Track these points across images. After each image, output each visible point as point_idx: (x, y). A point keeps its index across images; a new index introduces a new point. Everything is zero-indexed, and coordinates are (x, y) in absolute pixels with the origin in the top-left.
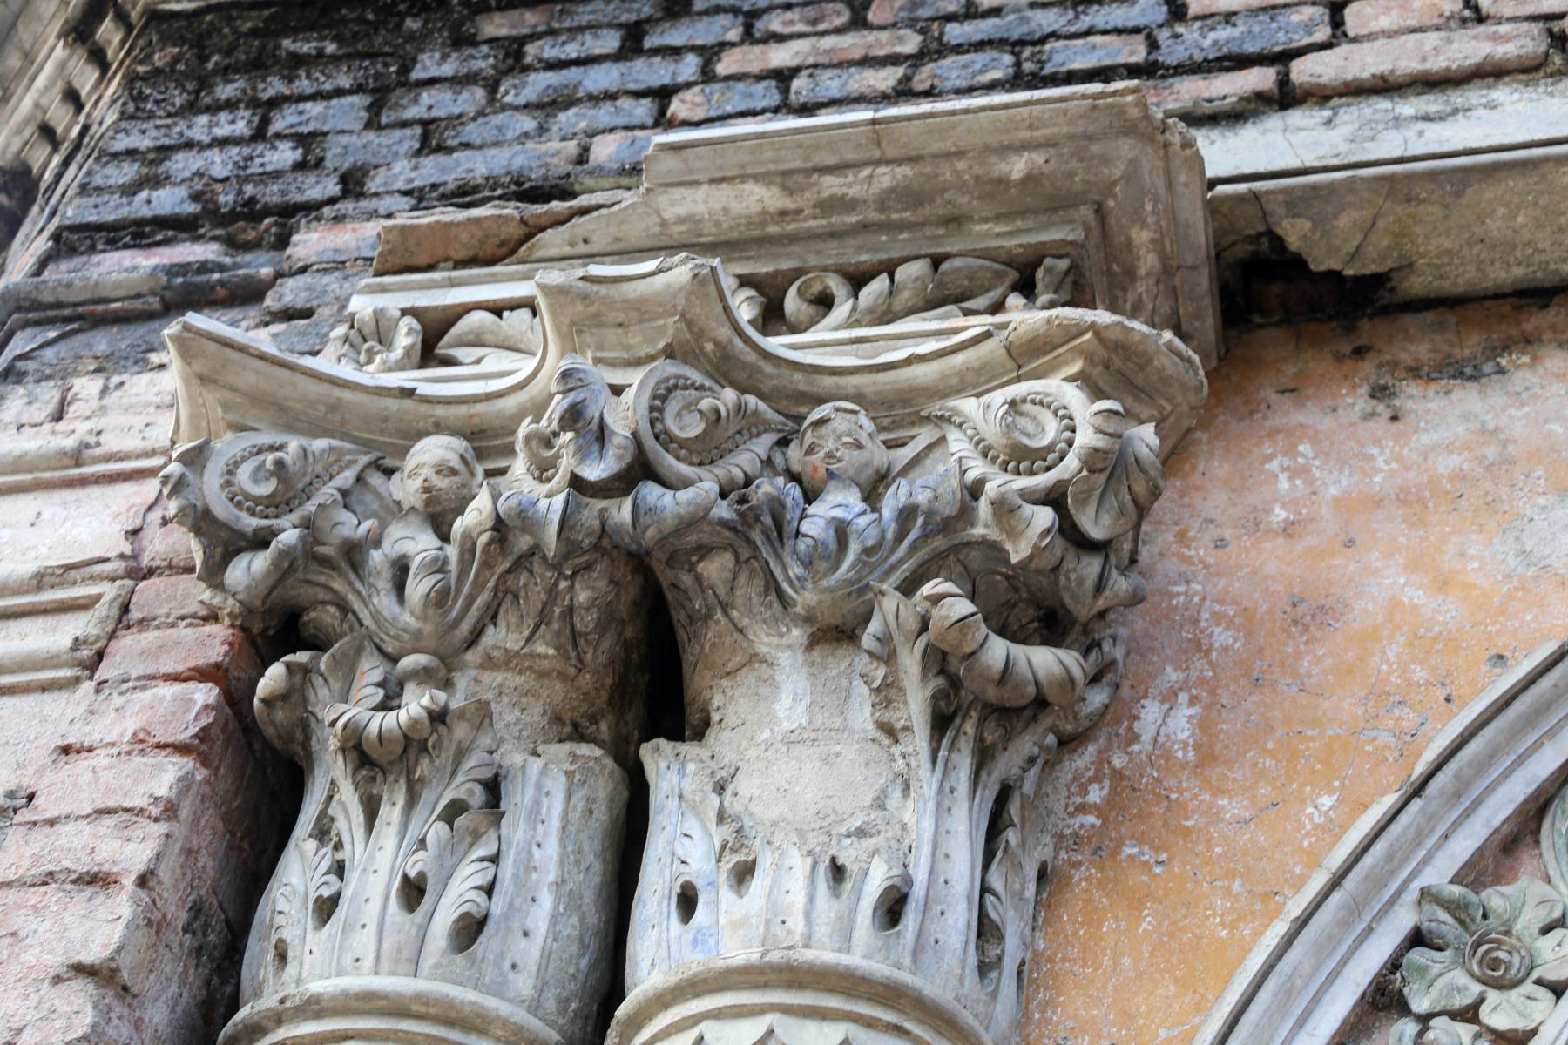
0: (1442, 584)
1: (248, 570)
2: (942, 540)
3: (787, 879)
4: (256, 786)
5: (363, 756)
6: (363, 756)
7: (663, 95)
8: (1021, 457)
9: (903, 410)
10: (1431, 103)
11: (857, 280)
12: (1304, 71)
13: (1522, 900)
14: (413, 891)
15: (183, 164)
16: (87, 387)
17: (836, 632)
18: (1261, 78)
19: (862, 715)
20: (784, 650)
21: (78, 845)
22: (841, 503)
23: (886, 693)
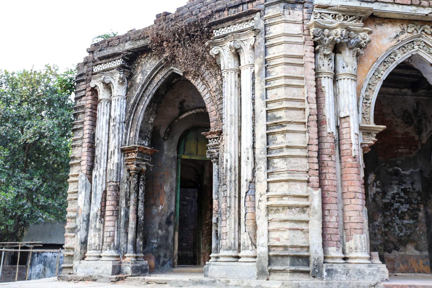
0: (378, 44)
8: (364, 39)
10: (384, 4)
11: (350, 16)
14: (328, 65)
16: (291, 11)
19: (352, 55)
20: (347, 49)
23: (353, 54)
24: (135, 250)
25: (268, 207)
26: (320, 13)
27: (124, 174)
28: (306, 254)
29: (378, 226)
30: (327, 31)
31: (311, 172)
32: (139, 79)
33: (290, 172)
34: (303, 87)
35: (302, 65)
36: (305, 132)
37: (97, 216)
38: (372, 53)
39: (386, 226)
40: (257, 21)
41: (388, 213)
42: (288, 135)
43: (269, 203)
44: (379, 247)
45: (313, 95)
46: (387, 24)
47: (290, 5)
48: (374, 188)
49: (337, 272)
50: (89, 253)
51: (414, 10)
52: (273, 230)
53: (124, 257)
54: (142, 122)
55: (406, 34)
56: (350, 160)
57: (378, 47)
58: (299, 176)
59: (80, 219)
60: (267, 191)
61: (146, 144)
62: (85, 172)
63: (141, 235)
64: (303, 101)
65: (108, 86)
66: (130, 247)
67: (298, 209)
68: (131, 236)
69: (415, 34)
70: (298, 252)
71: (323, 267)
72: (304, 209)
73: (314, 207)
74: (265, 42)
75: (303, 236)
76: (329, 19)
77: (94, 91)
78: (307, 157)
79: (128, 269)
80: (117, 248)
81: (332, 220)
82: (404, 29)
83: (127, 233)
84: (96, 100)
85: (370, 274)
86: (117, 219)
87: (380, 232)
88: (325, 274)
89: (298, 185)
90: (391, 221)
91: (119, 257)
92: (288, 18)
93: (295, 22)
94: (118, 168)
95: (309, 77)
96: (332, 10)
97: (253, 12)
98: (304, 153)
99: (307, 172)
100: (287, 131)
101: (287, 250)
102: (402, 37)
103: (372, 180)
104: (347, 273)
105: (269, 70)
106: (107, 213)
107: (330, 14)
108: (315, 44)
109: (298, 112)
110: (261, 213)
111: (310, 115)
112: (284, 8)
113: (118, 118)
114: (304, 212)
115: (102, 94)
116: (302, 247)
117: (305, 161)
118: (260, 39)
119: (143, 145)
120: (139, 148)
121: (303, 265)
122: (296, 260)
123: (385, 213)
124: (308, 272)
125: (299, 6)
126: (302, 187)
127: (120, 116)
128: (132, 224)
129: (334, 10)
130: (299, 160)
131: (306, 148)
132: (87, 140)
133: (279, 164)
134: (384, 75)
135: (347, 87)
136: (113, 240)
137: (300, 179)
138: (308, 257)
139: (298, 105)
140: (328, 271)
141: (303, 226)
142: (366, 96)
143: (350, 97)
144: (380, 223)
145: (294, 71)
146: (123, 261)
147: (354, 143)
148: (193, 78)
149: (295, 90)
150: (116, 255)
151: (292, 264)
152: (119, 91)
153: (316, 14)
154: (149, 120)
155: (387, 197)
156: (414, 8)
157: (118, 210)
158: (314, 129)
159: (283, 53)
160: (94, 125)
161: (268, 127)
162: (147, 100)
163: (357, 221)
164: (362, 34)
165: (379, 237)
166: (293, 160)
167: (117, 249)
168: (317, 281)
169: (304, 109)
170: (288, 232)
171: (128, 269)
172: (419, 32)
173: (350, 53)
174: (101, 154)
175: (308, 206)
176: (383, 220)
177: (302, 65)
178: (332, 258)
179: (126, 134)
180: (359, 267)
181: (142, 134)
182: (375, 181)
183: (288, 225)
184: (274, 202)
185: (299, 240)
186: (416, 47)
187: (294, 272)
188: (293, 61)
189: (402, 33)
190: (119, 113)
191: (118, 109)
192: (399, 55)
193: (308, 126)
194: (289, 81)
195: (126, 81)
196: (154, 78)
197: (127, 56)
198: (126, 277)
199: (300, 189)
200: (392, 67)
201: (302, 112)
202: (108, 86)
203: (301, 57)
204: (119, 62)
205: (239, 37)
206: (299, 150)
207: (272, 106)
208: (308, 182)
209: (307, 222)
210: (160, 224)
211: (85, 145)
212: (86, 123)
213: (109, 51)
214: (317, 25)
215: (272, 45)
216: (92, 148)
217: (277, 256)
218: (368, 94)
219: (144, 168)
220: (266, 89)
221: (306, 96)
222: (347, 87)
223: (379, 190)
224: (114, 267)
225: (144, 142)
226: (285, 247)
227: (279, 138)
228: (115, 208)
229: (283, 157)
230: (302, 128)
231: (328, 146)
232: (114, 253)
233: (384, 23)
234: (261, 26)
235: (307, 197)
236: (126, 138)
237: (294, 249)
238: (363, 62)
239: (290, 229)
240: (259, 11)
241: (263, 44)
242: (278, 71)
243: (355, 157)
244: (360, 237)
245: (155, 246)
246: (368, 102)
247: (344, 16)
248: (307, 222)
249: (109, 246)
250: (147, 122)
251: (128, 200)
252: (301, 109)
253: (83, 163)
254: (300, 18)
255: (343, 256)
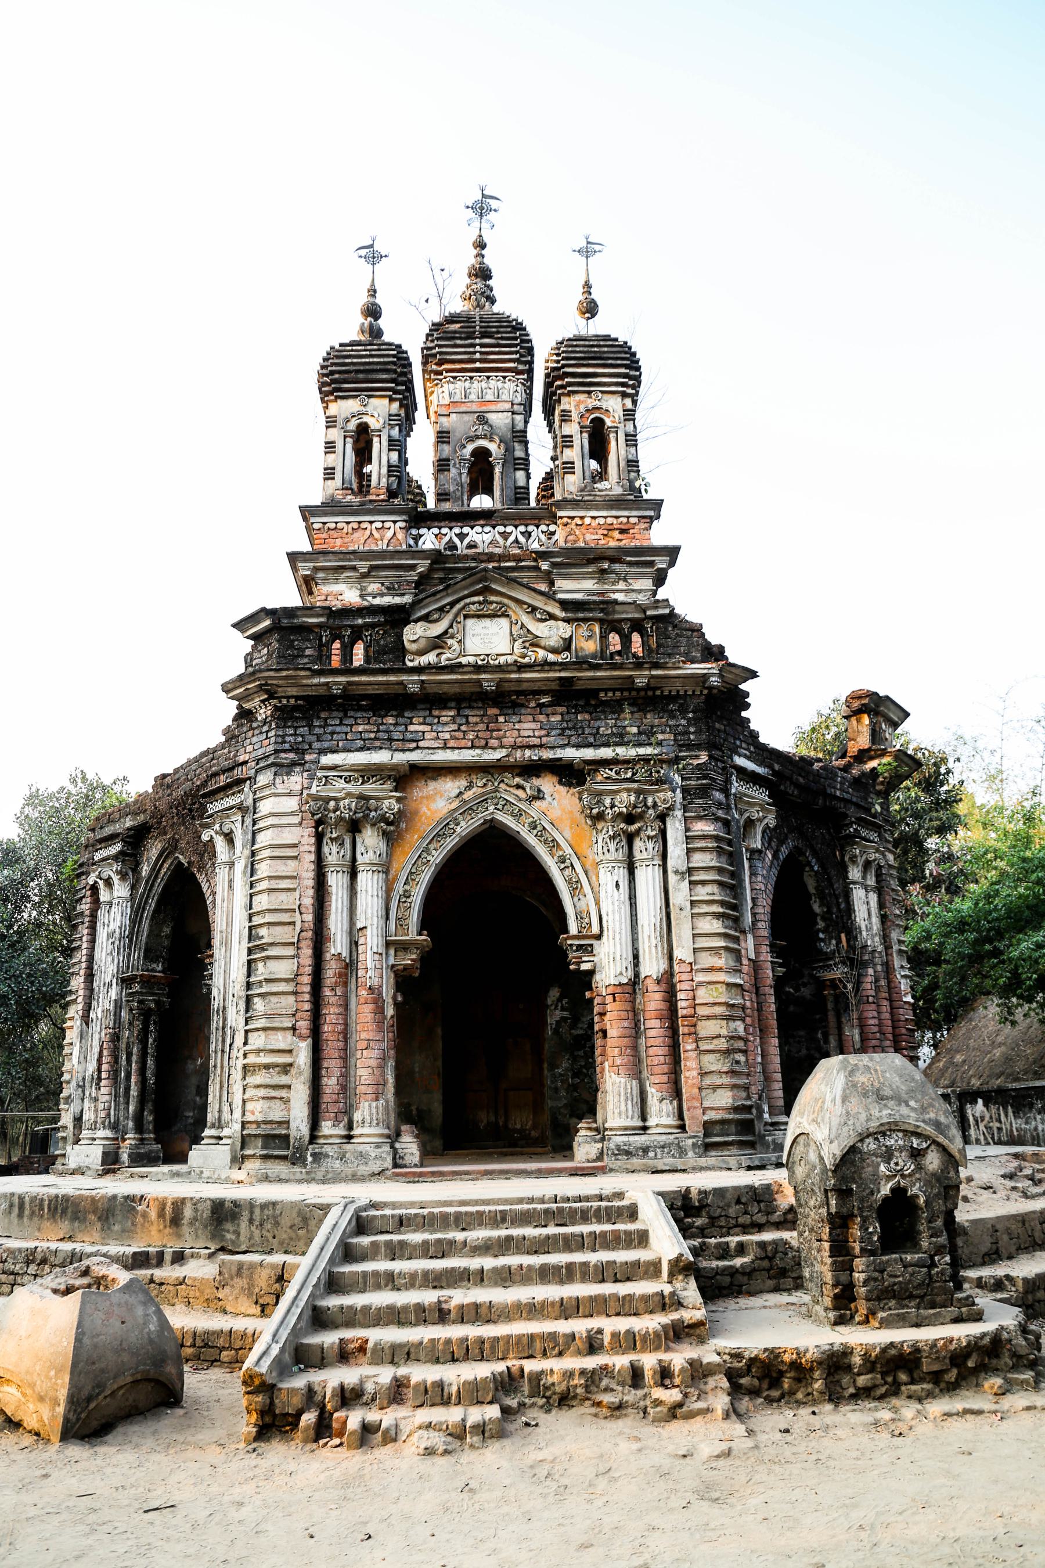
1: (317, 817)
2: (383, 819)
3: (371, 853)
4: (319, 838)
5: (331, 838)
6: (331, 838)
7: (346, 733)
9: (378, 799)
10: (430, 751)
11: (373, 776)
12: (421, 744)
13: (431, 847)
15: (288, 739)
16: (285, 778)
17: (373, 825)
18: (414, 745)
21: (307, 848)
22: (373, 814)
24: (139, 1128)
25: (245, 1067)
26: (326, 777)
27: (124, 1014)
28: (284, 1132)
29: (561, 1075)
30: (332, 804)
31: (299, 1014)
32: (145, 870)
33: (269, 1016)
34: (294, 890)
35: (295, 858)
36: (293, 957)
37: (93, 1078)
38: (419, 824)
39: (575, 1075)
40: (246, 796)
41: (581, 1053)
42: (270, 963)
43: (246, 1061)
44: (562, 1110)
45: (308, 901)
46: (445, 776)
47: (285, 770)
48: (558, 1012)
49: (327, 1156)
50: (85, 1133)
51: (478, 755)
52: (251, 1100)
53: (124, 1140)
54: (148, 936)
55: (474, 789)
56: (364, 993)
57: (429, 813)
58: (281, 1022)
59: (73, 1084)
60: (245, 1044)
61: (160, 968)
62: (80, 1013)
63: (150, 1106)
64: (294, 910)
65: (108, 883)
66: (131, 1124)
67: (277, 1069)
68: (131, 1108)
69: (489, 787)
70: (274, 1129)
71: (307, 1149)
72: (286, 1069)
73: (299, 1067)
74: (254, 824)
75: (283, 1107)
76: (341, 784)
77: (94, 888)
78: (295, 993)
79: (125, 1157)
80: (114, 1127)
81: (330, 1083)
82: (471, 782)
83: (128, 1103)
84: (96, 902)
85: (376, 1157)
86: (116, 1083)
87: (565, 1086)
88: (310, 1159)
89: (280, 1035)
90: (584, 1067)
91: (117, 1139)
92: (280, 788)
93: (289, 794)
94: (116, 1007)
95: (305, 875)
96: (343, 771)
97: (240, 782)
98: (290, 988)
99: (294, 1015)
100: (268, 957)
101: (259, 1127)
102: (468, 795)
103: (555, 999)
104: (342, 1157)
105: (256, 866)
106: (104, 1075)
107: (341, 777)
108: (319, 823)
109: (286, 927)
110: (237, 1075)
111: (302, 931)
112: (275, 774)
113: (118, 930)
114: (286, 1073)
115: (104, 896)
116: (280, 1123)
117: (291, 999)
118: (248, 821)
119: (153, 970)
120: (141, 976)
121: (280, 1148)
122: (271, 1141)
123: (576, 1053)
124: (284, 1158)
125: (298, 769)
126: (285, 1037)
127: (120, 928)
128: (134, 1092)
129: (347, 771)
130: (283, 997)
131: (292, 980)
132: (84, 965)
133: (259, 1004)
134: (437, 857)
135: (369, 883)
136: (109, 1115)
137: (281, 1025)
138: (287, 1136)
139: (285, 917)
140: (314, 1155)
141: (283, 1093)
142: (405, 891)
143: (369, 898)
144: (566, 1069)
145: (283, 868)
146: (122, 1145)
147: (373, 967)
148: (198, 871)
149: (283, 896)
150: (111, 1136)
151: (263, 1148)
152: (121, 890)
153: (321, 779)
154: (161, 931)
155: (580, 1025)
156: (478, 751)
157: (117, 1070)
158: (307, 952)
159: (267, 843)
160: (93, 941)
161: (250, 951)
162: (152, 904)
163: (368, 1082)
164: (386, 802)
165: (563, 1093)
166: (274, 999)
167: (114, 1128)
168: (297, 1169)
169: (293, 923)
170: (261, 1101)
171: (125, 1157)
172: (496, 784)
173: (373, 832)
174: (99, 986)
175: (291, 1065)
176: (572, 1065)
177: (295, 858)
178: (326, 1137)
179: (129, 955)
180: (361, 1148)
181: (150, 954)
182: (560, 1000)
183: (262, 1092)
184: (252, 1059)
185: (277, 1115)
186: (491, 808)
187: (265, 1157)
188: (285, 852)
189: (469, 787)
190: (119, 924)
191: (114, 919)
192: (463, 823)
193: (298, 948)
194: (274, 884)
195: (131, 873)
196: (160, 870)
197: (128, 837)
198: (119, 1169)
199: (282, 1040)
200: (450, 843)
201: (292, 927)
202: (108, 883)
203: (295, 846)
204: (117, 847)
205: (228, 817)
206: (284, 984)
207: (257, 920)
208: (294, 1028)
209: (289, 1087)
210: (198, 1086)
211: (82, 972)
212: (85, 939)
213: (108, 831)
214: (315, 798)
215: (260, 830)
216: (90, 977)
217: (249, 1135)
218: (407, 887)
219: (153, 1005)
220: (251, 896)
221: (298, 903)
222: (369, 883)
223: (566, 1014)
224: (105, 1154)
225: (154, 965)
226: (258, 1123)
227: (260, 965)
228: (112, 1067)
229: (260, 995)
230: (291, 951)
231: (330, 975)
232: (109, 1133)
233: (440, 775)
234: (250, 802)
235: (290, 1051)
236: (129, 961)
237: (269, 1126)
238: (402, 839)
239: (263, 1098)
240: (249, 778)
241: (250, 828)
242: (263, 869)
243: (370, 988)
244: (370, 1105)
245: (191, 1121)
246: (409, 900)
247: (363, 777)
248: (289, 1087)
249: (103, 1123)
250: (158, 935)
251: (129, 1055)
252: (290, 923)
253: (80, 999)
254: (299, 787)
255: (640, 1124)
